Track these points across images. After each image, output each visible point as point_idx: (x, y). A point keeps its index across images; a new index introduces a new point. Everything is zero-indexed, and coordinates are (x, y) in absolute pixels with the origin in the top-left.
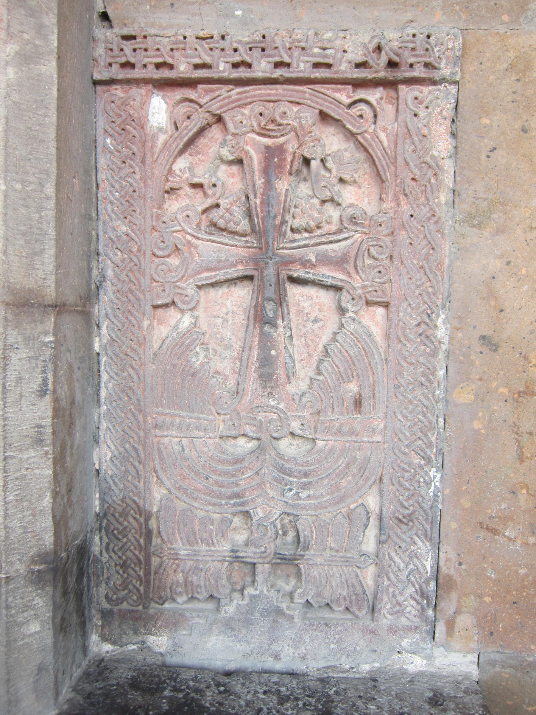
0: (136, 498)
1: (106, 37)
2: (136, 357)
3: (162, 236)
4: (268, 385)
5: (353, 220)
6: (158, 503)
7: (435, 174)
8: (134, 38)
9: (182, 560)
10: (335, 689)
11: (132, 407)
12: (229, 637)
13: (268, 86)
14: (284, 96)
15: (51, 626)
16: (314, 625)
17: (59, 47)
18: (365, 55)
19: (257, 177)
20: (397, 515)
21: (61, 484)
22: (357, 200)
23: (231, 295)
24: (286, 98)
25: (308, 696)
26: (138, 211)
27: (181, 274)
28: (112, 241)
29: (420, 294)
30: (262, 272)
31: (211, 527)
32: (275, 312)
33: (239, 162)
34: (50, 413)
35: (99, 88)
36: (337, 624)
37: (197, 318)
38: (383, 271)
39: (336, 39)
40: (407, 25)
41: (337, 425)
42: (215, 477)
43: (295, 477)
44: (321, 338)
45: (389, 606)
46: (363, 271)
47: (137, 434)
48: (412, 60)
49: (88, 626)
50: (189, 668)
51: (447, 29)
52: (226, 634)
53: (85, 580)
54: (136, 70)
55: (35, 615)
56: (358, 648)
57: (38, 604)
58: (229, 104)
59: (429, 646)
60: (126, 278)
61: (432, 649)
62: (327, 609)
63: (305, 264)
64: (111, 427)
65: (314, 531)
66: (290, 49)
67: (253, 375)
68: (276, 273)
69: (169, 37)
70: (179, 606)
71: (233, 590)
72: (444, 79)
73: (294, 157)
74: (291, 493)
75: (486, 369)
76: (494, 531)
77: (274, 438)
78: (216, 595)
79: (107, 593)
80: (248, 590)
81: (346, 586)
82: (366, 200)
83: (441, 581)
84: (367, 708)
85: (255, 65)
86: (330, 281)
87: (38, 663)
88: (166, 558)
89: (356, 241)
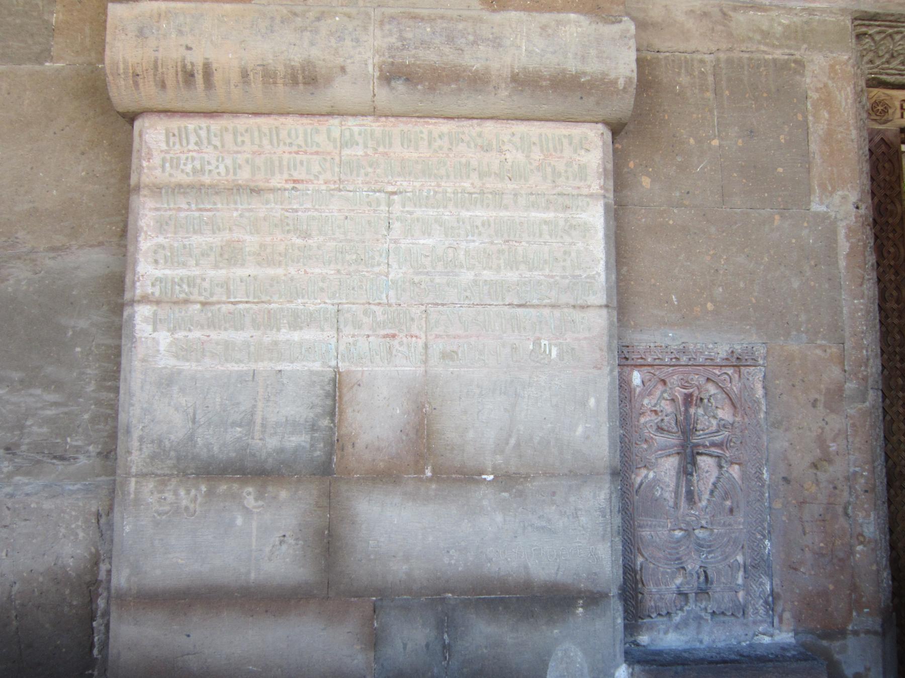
5: (724, 426)
8: (628, 347)
32: (692, 469)
45: (752, 610)
48: (747, 357)
63: (705, 446)
67: (683, 499)
76: (795, 569)
78: (670, 611)
83: (775, 595)
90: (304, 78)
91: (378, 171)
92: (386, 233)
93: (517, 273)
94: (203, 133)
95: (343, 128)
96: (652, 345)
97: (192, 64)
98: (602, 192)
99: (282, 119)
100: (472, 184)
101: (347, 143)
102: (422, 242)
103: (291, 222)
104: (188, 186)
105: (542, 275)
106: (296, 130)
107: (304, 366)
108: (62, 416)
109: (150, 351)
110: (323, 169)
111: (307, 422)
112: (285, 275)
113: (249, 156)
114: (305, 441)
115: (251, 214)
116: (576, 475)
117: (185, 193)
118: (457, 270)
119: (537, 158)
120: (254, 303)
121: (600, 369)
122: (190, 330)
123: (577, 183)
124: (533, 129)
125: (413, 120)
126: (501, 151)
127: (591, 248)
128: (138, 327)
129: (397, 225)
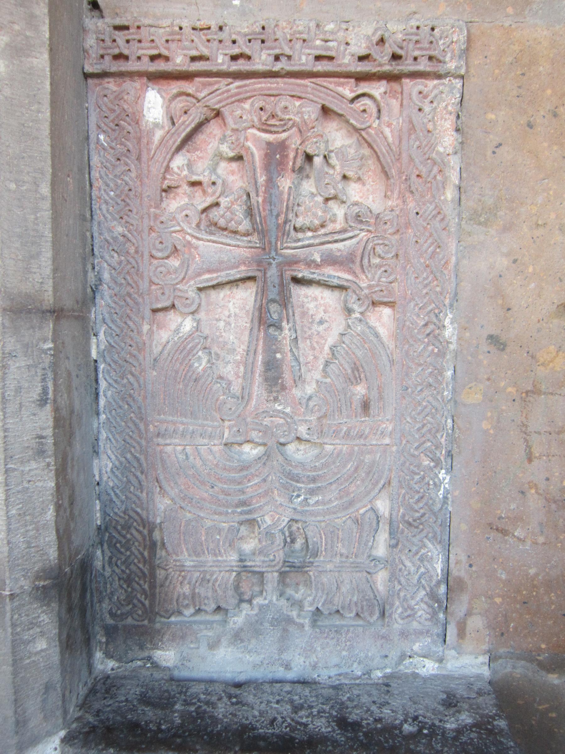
0: (139, 510)
1: (97, 27)
2: (135, 363)
3: (161, 237)
4: (274, 389)
6: (163, 515)
7: (440, 171)
8: (127, 28)
9: (189, 571)
10: (348, 695)
11: (132, 415)
12: (238, 649)
13: (269, 79)
14: (285, 90)
15: (58, 643)
16: (324, 633)
17: (51, 39)
18: (368, 47)
19: (259, 175)
20: (406, 518)
21: (64, 496)
22: (361, 197)
23: (233, 298)
24: (287, 93)
25: (323, 704)
26: (135, 211)
28: (108, 243)
29: (427, 293)
30: (265, 273)
31: (218, 537)
33: (239, 158)
34: (51, 423)
35: (90, 81)
36: (348, 631)
37: (198, 322)
38: (390, 270)
39: (338, 31)
40: (411, 16)
41: (345, 429)
42: (220, 485)
43: (303, 482)
44: (326, 340)
45: (400, 610)
46: (368, 271)
47: (139, 443)
48: (417, 53)
49: (93, 643)
50: (199, 681)
51: (452, 21)
52: (235, 645)
53: (88, 595)
54: (130, 62)
55: (41, 632)
56: (370, 654)
57: (43, 621)
58: (228, 98)
59: (441, 649)
60: (123, 281)
61: (443, 651)
62: (337, 616)
63: (311, 264)
64: (111, 437)
65: (323, 537)
66: (291, 41)
67: (258, 379)
68: (280, 274)
69: (164, 28)
70: (186, 619)
71: (241, 601)
72: (449, 73)
73: (297, 153)
74: (299, 499)
75: (494, 369)
77: (281, 444)
78: (223, 605)
79: (111, 608)
80: (257, 600)
81: (356, 592)
82: (371, 197)
84: (382, 712)
85: (255, 57)
86: (336, 282)
87: (45, 681)
88: (171, 570)
89: (361, 240)
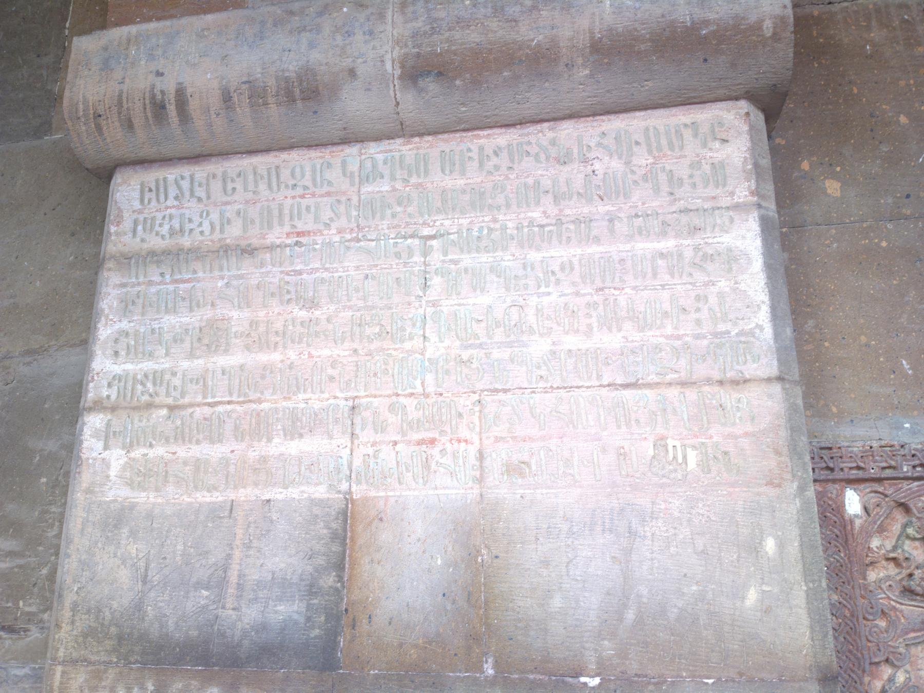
8: (830, 449)
27: (892, 635)
58: (909, 495)
90: (302, 92)
91: (410, 209)
92: (421, 294)
93: (620, 335)
94: (185, 184)
95: (363, 157)
96: (875, 444)
97: (163, 92)
98: (756, 199)
99: (284, 155)
100: (544, 212)
101: (368, 177)
102: (471, 301)
103: (292, 288)
104: (163, 253)
105: (662, 336)
106: (302, 167)
107: (303, 492)
108: (16, 570)
109: (98, 478)
110: (336, 214)
111: (302, 580)
112: (282, 361)
113: (241, 206)
114: (297, 612)
115: (241, 281)
116: (751, 680)
117: (159, 263)
118: (524, 338)
119: (644, 162)
120: (238, 403)
121: (779, 486)
122: (151, 446)
123: (711, 191)
124: (635, 122)
125: (458, 135)
126: (585, 161)
127: (742, 286)
128: (85, 444)
129: (436, 281)
